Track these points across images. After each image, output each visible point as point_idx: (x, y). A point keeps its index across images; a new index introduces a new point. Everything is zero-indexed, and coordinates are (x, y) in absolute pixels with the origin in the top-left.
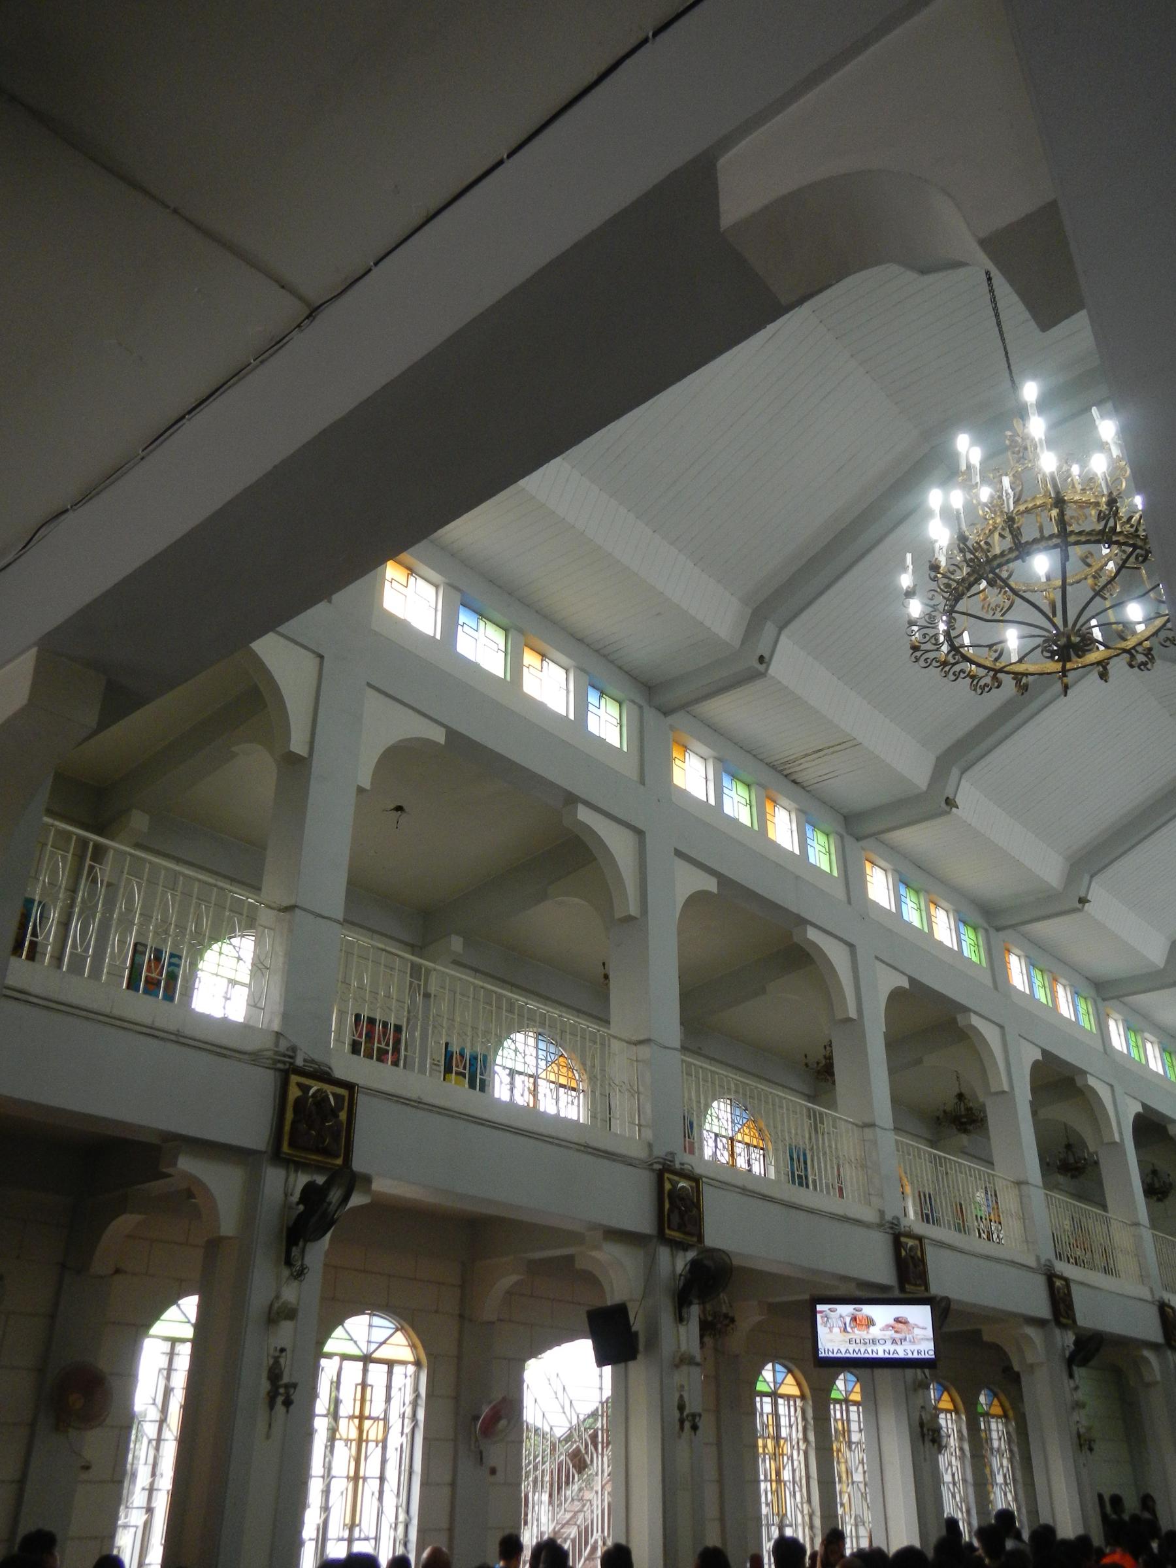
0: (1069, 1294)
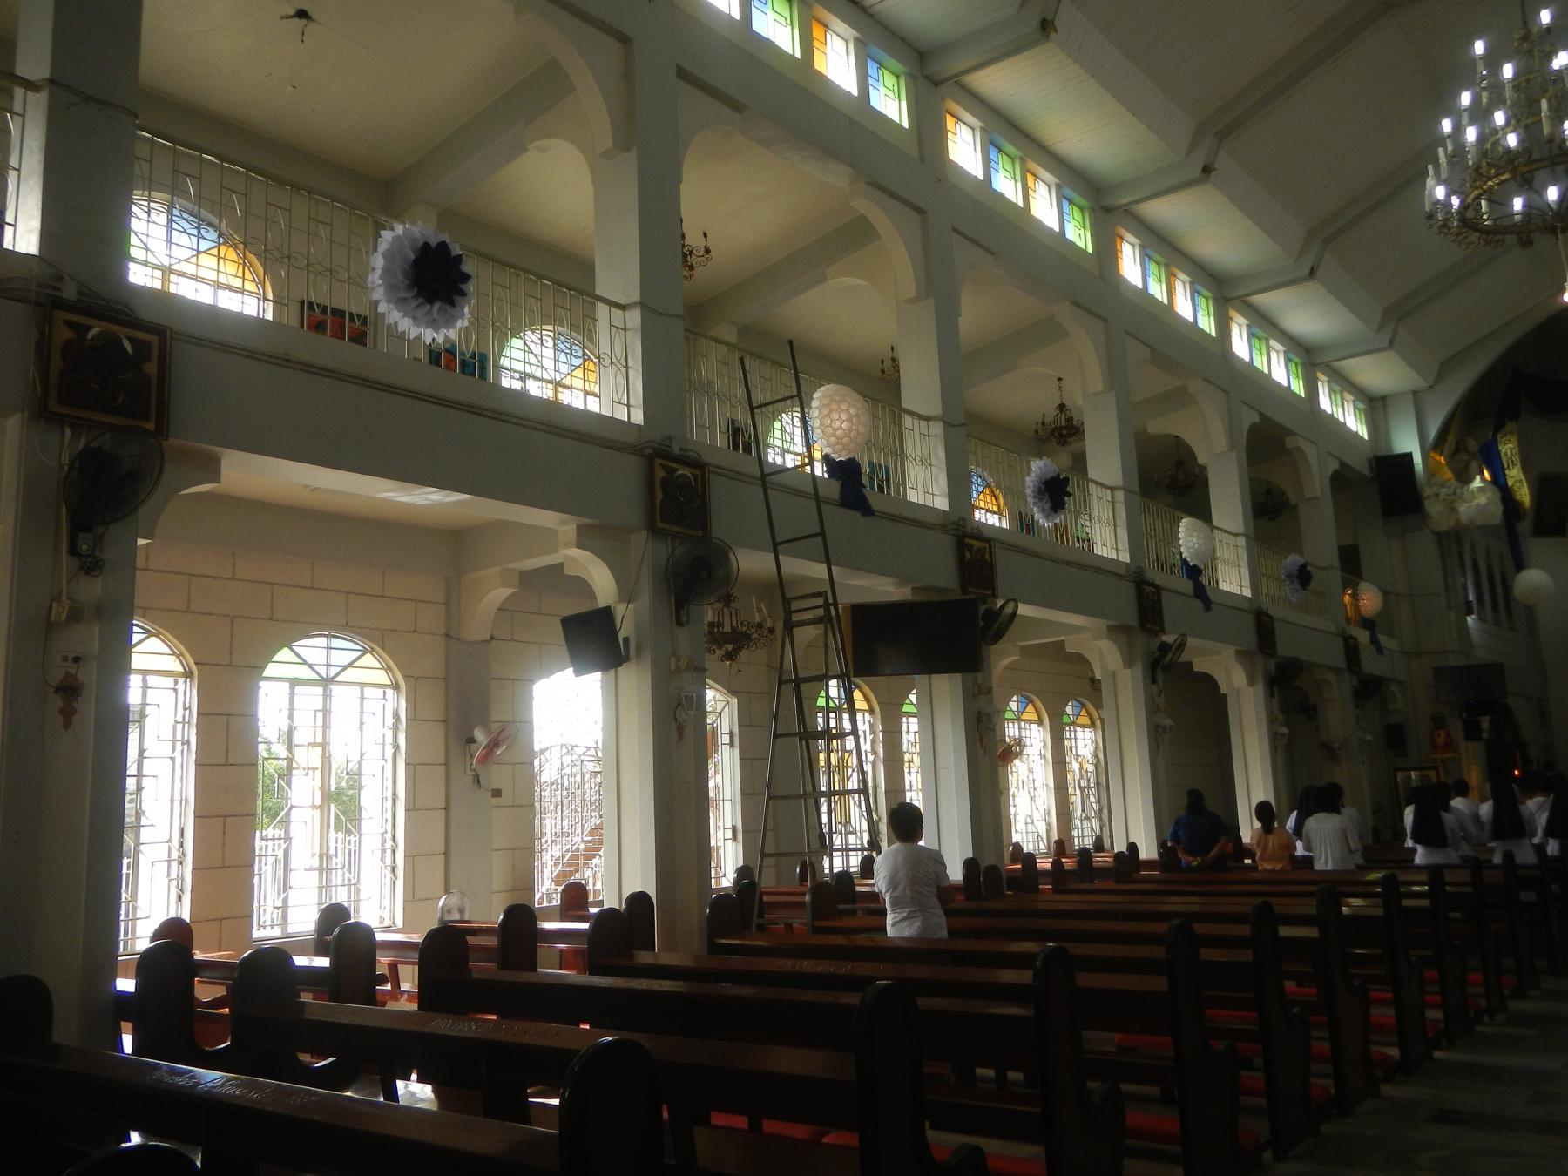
0: (1159, 602)
